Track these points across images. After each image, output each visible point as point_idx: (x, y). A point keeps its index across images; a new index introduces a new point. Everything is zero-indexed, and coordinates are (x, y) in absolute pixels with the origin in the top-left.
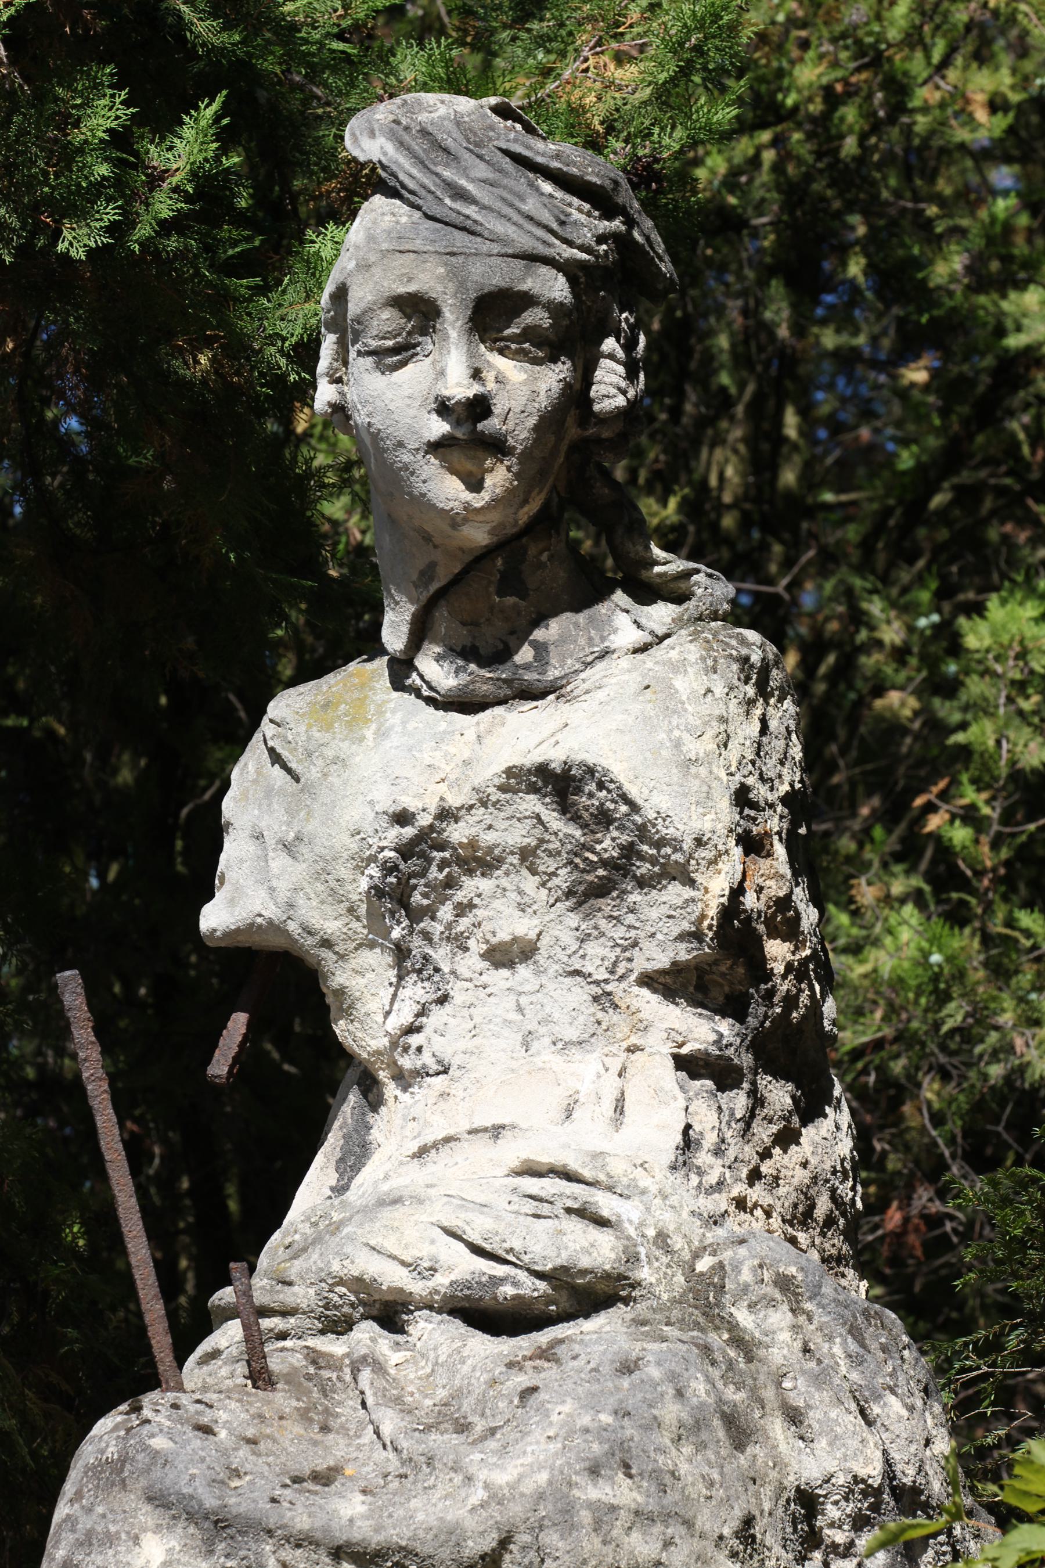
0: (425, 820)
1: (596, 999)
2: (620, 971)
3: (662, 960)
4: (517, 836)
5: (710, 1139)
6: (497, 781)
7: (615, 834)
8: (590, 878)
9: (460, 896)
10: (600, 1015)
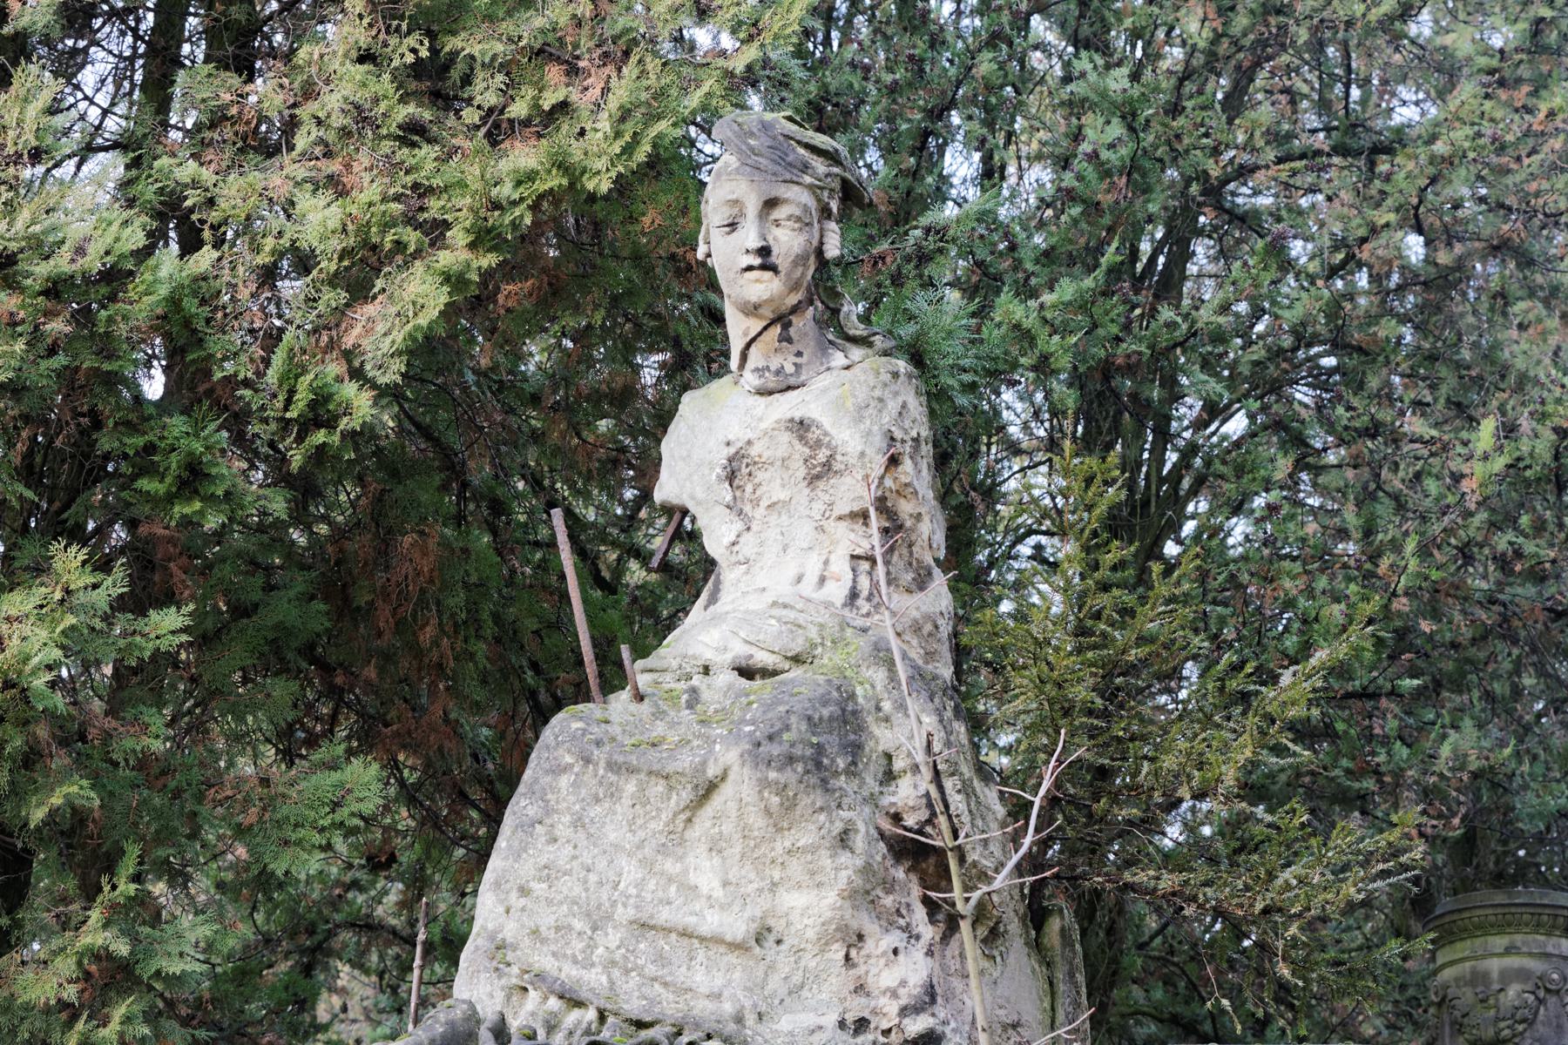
0: (740, 445)
4: (781, 451)
5: (865, 593)
9: (756, 481)
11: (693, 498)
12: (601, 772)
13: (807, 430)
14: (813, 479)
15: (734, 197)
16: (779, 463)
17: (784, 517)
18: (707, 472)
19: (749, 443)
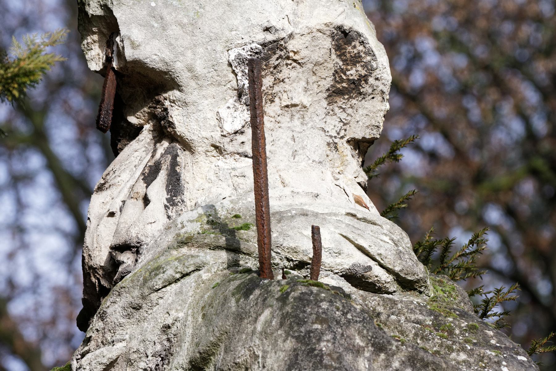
0: (283, 35)
1: (329, 144)
4: (317, 56)
6: (318, 27)
7: (360, 68)
8: (338, 86)
9: (280, 76)
10: (329, 152)
11: (190, 69)
12: (396, 364)
13: (349, 43)
14: (334, 94)
16: (310, 66)
17: (297, 122)
18: (219, 48)
19: (291, 36)
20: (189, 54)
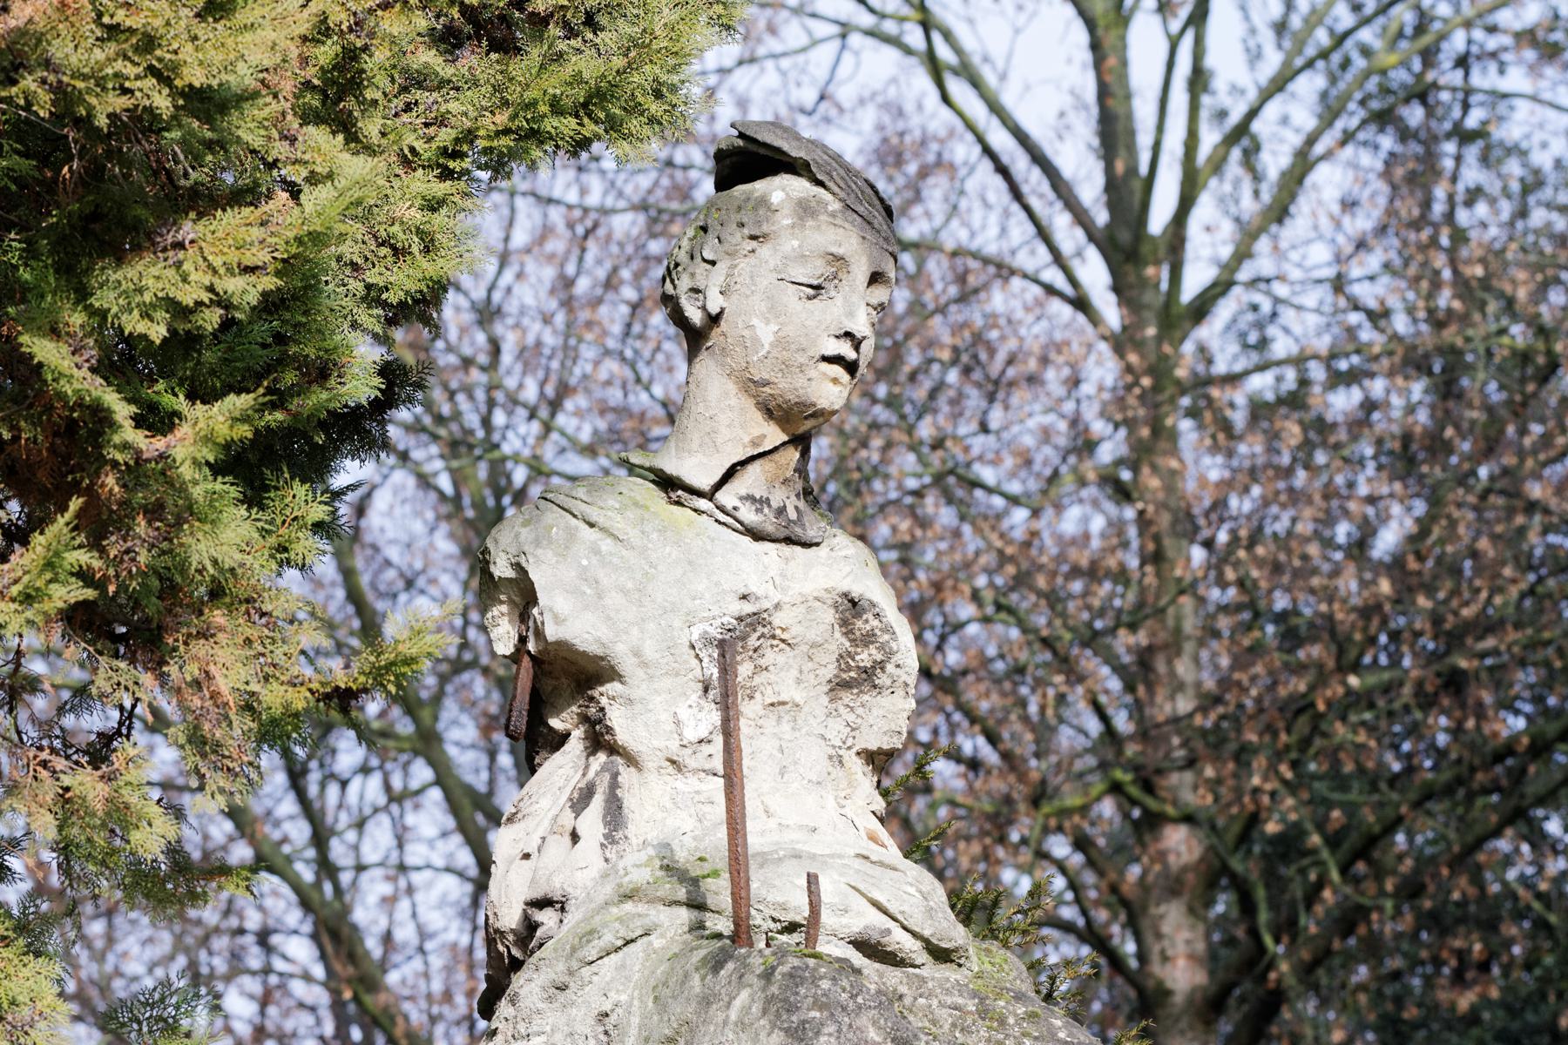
2: (850, 742)
3: (873, 746)
4: (813, 634)
9: (763, 662)
11: (637, 653)
13: (858, 615)
14: (840, 685)
15: (840, 251)
16: (805, 648)
18: (677, 623)
19: (777, 606)
20: (635, 631)
